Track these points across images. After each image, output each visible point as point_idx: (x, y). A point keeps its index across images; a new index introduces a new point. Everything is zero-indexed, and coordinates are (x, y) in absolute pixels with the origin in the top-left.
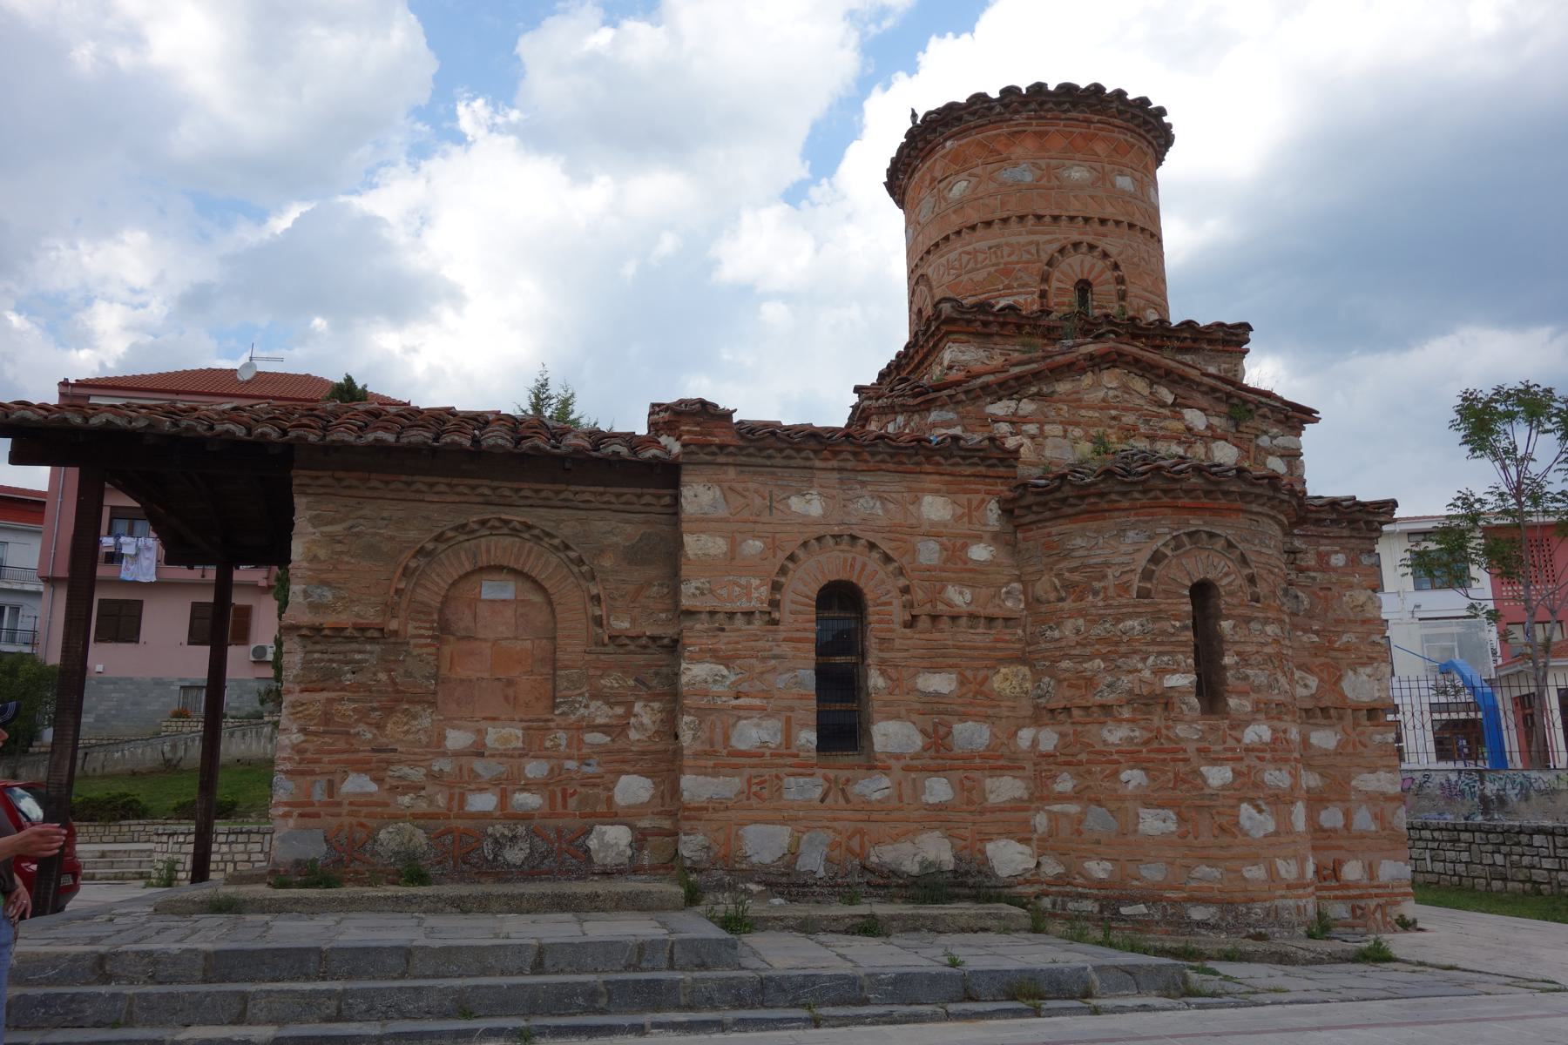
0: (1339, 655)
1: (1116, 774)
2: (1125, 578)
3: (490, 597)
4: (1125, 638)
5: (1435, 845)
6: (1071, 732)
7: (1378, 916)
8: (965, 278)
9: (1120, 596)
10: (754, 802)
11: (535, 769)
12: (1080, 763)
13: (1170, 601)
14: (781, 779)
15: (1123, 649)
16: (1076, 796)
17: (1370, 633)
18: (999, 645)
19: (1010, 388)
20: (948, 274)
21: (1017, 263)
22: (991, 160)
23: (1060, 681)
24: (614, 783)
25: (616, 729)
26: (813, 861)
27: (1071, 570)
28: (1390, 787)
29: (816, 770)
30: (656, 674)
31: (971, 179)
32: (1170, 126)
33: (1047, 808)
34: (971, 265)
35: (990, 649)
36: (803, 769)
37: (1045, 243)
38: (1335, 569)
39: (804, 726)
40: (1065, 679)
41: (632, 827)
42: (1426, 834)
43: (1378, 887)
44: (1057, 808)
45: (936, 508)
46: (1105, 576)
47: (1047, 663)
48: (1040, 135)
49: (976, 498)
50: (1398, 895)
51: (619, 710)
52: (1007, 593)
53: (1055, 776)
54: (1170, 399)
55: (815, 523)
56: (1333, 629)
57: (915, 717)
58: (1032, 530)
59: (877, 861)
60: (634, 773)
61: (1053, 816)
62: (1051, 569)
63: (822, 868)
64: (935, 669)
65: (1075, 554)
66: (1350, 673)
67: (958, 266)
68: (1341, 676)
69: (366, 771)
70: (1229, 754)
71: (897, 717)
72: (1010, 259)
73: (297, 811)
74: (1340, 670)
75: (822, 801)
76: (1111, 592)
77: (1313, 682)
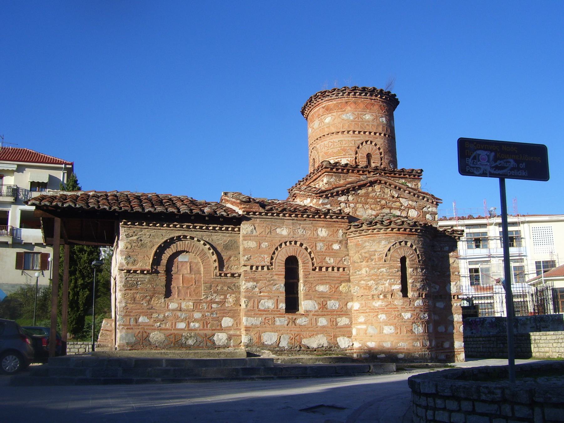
1: (377, 315)
2: (381, 256)
3: (181, 260)
4: (381, 274)
5: (483, 342)
6: (364, 303)
8: (330, 151)
9: (379, 261)
10: (267, 325)
11: (197, 315)
12: (367, 312)
13: (394, 263)
14: (275, 319)
15: (380, 277)
16: (365, 323)
18: (342, 276)
19: (345, 192)
20: (324, 149)
21: (348, 147)
22: (339, 110)
23: (361, 288)
24: (222, 319)
25: (222, 303)
26: (284, 344)
27: (365, 253)
29: (285, 315)
30: (234, 285)
31: (332, 116)
32: (398, 99)
33: (356, 327)
34: (332, 146)
35: (339, 277)
36: (281, 315)
37: (357, 140)
39: (281, 302)
40: (362, 287)
41: (228, 334)
42: (481, 339)
44: (359, 327)
45: (323, 233)
46: (375, 255)
47: (357, 282)
48: (355, 103)
49: (335, 229)
50: (460, 352)
51: (222, 297)
52: (344, 259)
53: (359, 317)
54: (396, 196)
55: (285, 237)
57: (316, 299)
58: (353, 239)
59: (304, 344)
60: (228, 317)
61: (358, 330)
62: (359, 252)
63: (287, 346)
64: (322, 284)
65: (366, 247)
67: (328, 146)
69: (146, 316)
70: (410, 309)
71: (311, 299)
72: (345, 146)
73: (126, 328)
75: (287, 325)
76: (377, 260)
77: (438, 287)
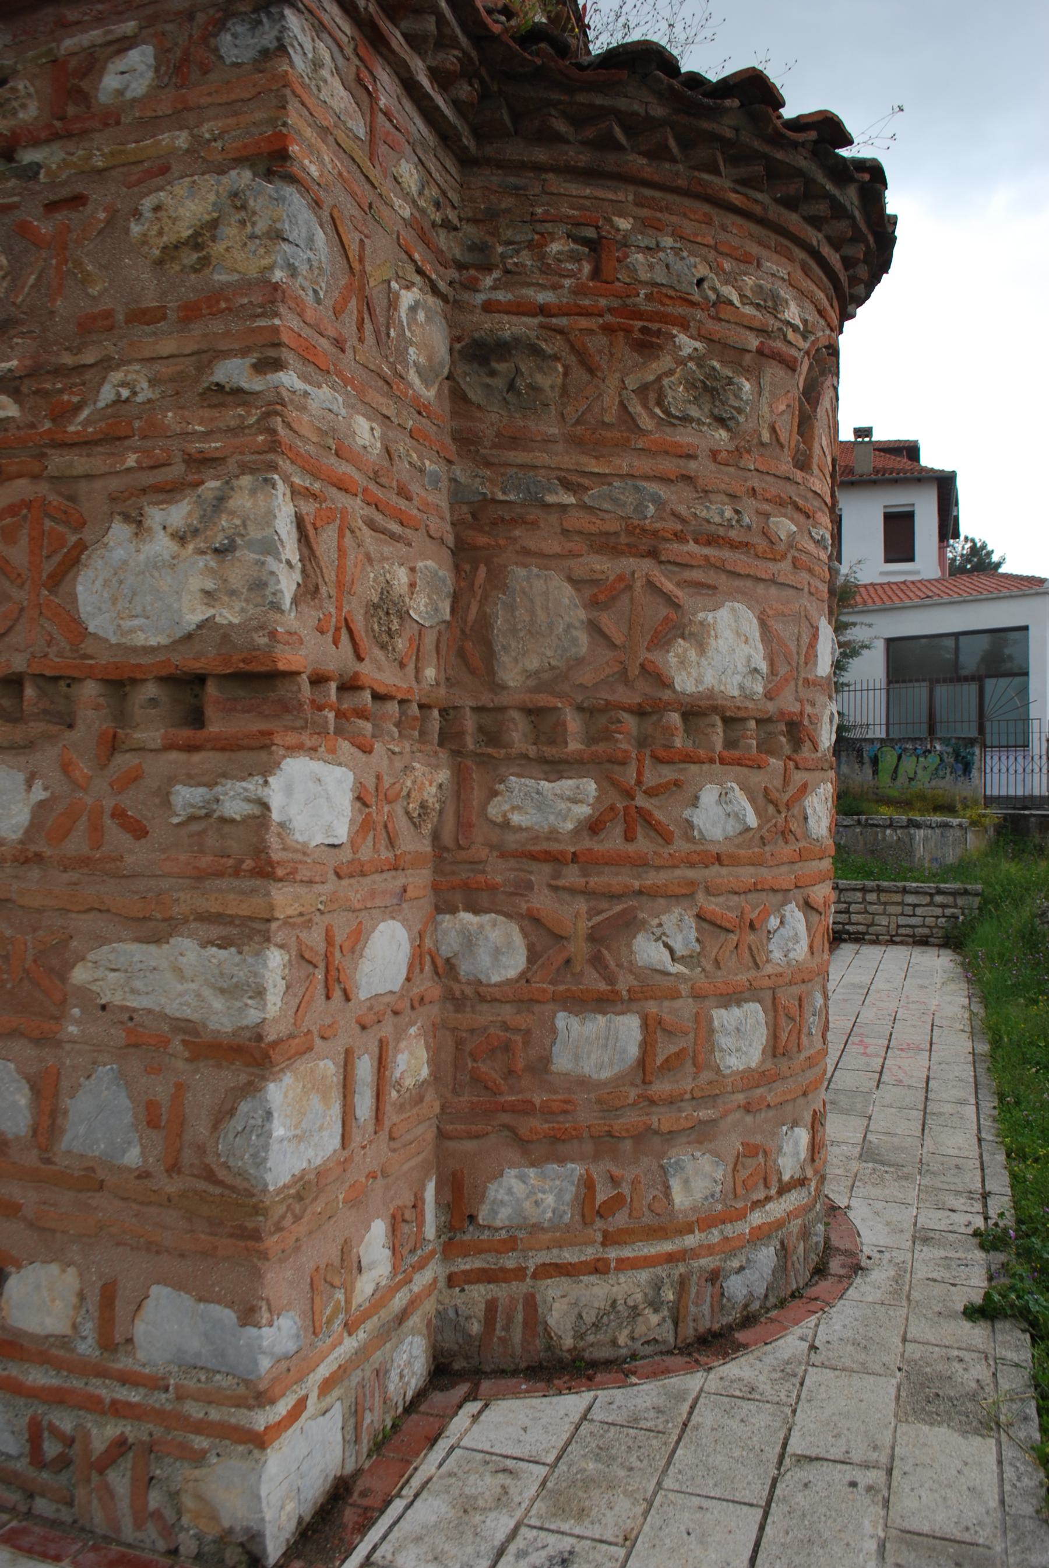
0: (79, 463)
7: (119, 1480)
17: (213, 355)
28: (218, 1004)
38: (110, 118)
43: (126, 1379)
56: (68, 359)
66: (120, 530)
68: (81, 547)
74: (80, 525)
